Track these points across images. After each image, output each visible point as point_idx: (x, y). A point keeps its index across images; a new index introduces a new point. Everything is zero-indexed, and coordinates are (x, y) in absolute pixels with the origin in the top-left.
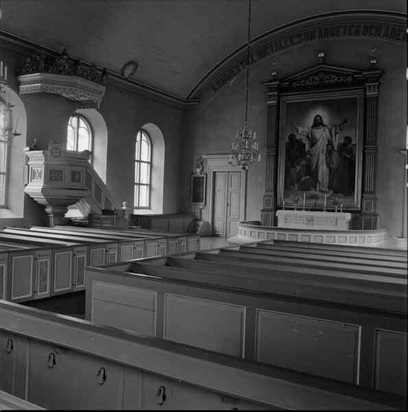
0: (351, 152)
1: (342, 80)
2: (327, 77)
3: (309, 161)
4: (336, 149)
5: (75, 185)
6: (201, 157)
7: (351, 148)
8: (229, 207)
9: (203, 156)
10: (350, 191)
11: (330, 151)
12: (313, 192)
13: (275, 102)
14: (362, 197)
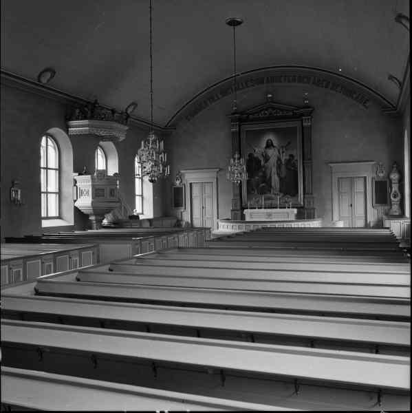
3: (264, 172)
4: (283, 163)
5: (112, 199)
6: (179, 172)
9: (182, 171)
10: (295, 193)
12: (269, 195)
14: (304, 197)
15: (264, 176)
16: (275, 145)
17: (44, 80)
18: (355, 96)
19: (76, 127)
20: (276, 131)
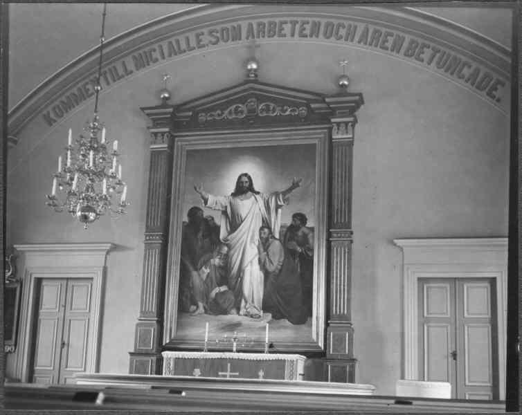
0: (305, 242)
1: (288, 113)
3: (227, 258)
4: (277, 236)
7: (305, 236)
8: (65, 350)
10: (302, 315)
11: (267, 239)
12: (233, 317)
13: (166, 146)
14: (327, 325)
15: (226, 267)
16: (256, 188)
18: (466, 71)
20: (267, 155)
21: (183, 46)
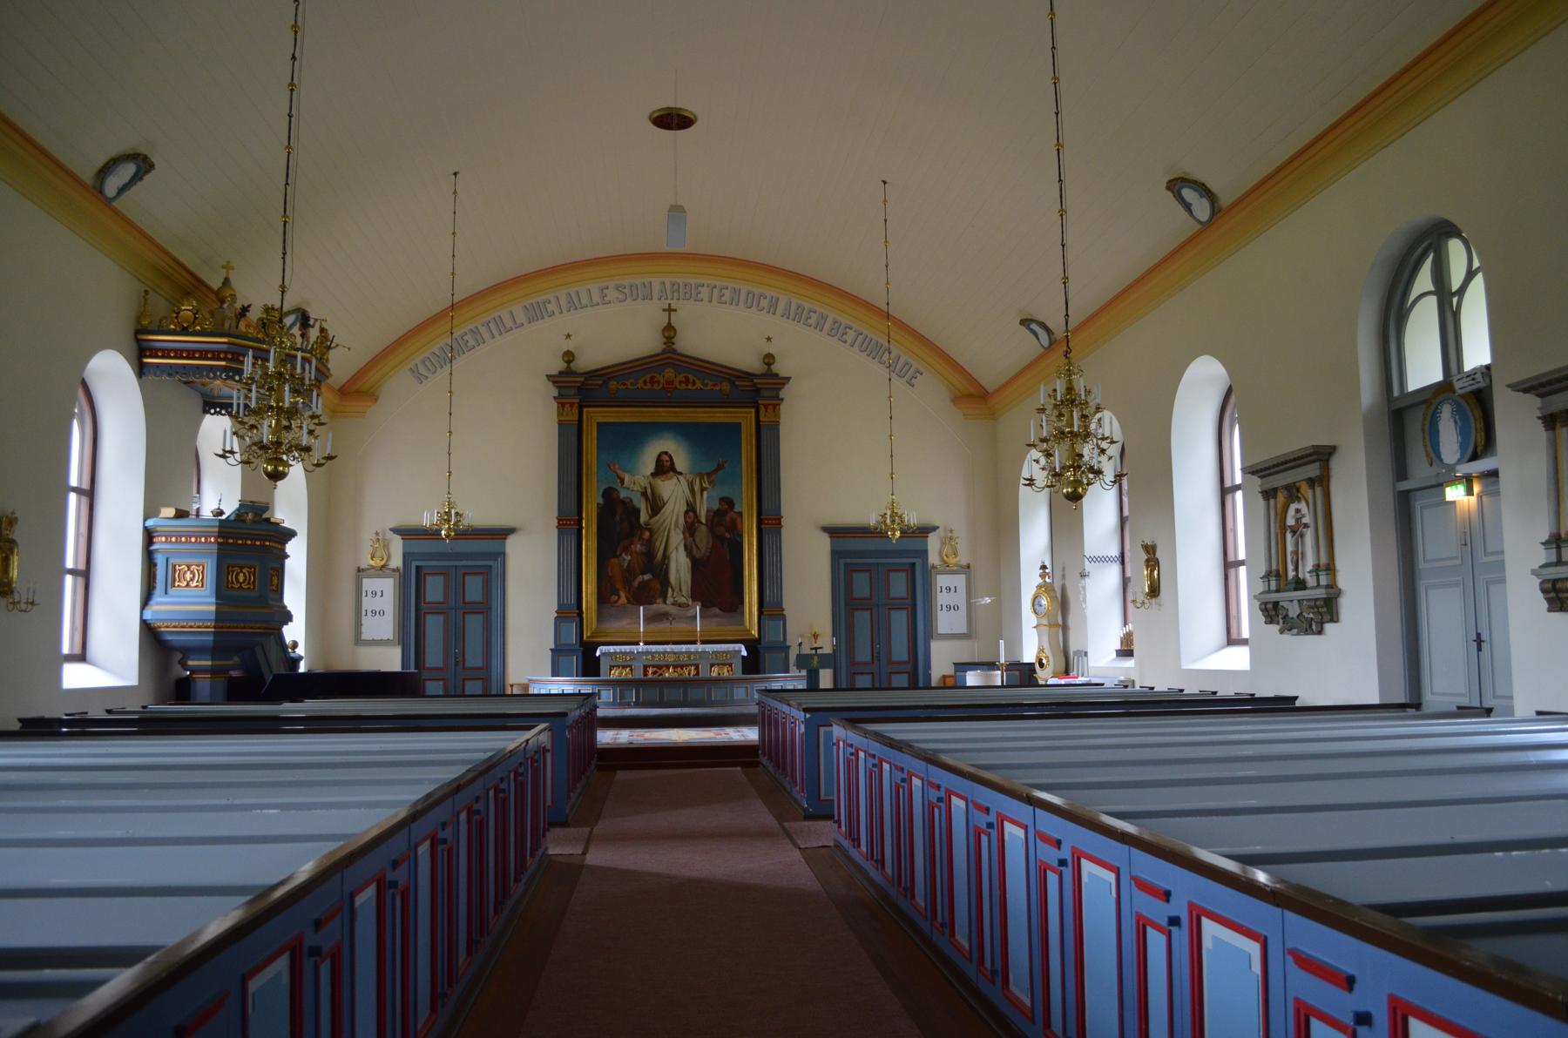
2: (681, 377)
7: (733, 521)
10: (731, 602)
11: (693, 524)
12: (659, 606)
15: (650, 553)
16: (679, 467)
17: (112, 185)
19: (166, 353)
20: (687, 432)
21: (585, 301)
